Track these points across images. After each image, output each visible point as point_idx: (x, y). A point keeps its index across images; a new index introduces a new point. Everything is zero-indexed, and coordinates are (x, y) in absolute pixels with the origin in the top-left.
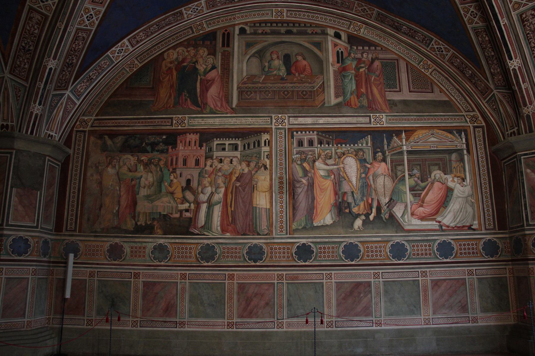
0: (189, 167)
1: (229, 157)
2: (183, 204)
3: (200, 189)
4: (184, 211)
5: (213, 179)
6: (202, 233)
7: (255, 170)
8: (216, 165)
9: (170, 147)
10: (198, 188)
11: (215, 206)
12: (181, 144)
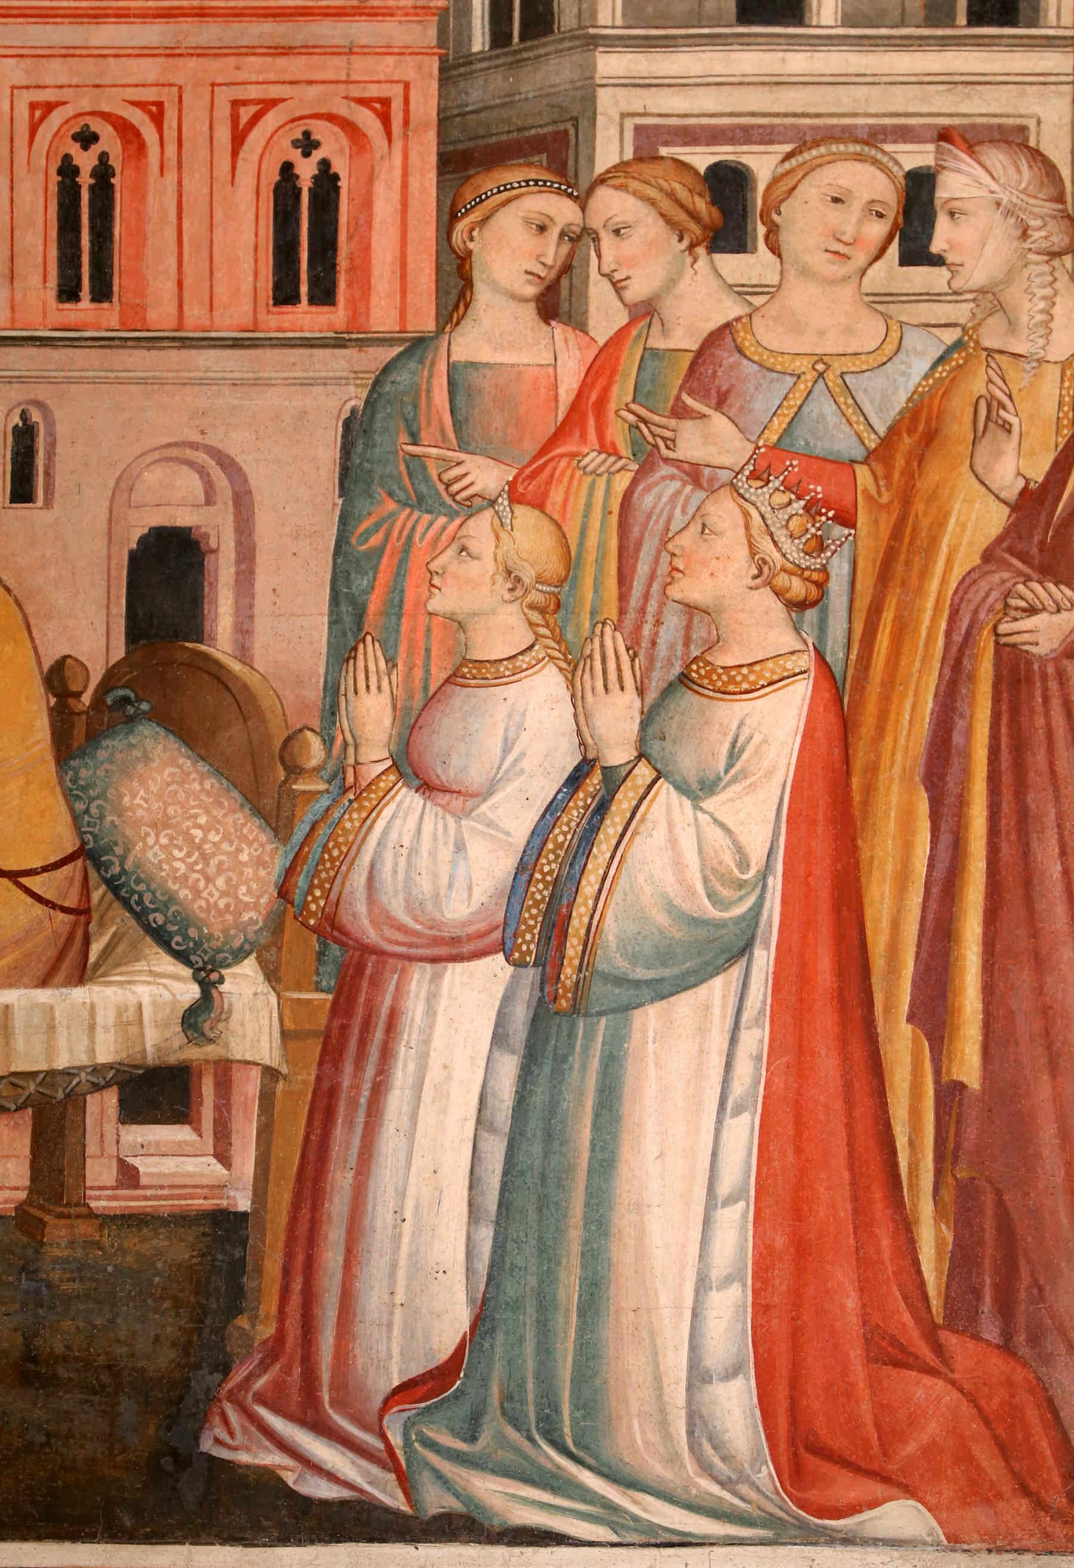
1: (875, 136)
2: (81, 975)
8: (637, 291)
10: (333, 691)
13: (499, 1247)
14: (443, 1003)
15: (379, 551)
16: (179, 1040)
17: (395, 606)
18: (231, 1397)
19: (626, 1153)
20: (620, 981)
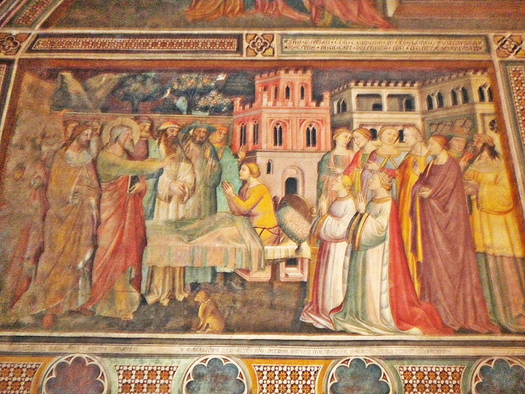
0: (289, 147)
2: (279, 243)
3: (324, 204)
4: (282, 265)
5: (358, 180)
6: (339, 328)
7: (467, 157)
8: (361, 146)
9: (238, 101)
10: (318, 202)
11: (370, 251)
12: (265, 95)
13: (348, 287)
14: (336, 249)
15: (323, 182)
16: (295, 254)
17: (327, 189)
18: (305, 312)
19: (367, 272)
20: (365, 246)
